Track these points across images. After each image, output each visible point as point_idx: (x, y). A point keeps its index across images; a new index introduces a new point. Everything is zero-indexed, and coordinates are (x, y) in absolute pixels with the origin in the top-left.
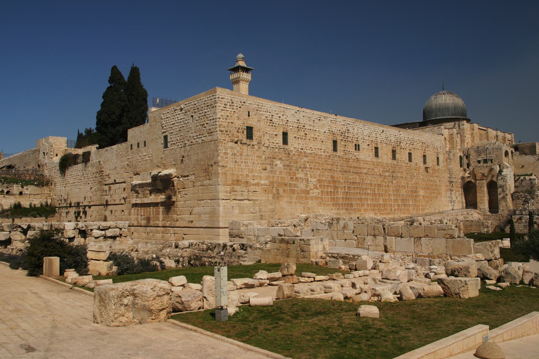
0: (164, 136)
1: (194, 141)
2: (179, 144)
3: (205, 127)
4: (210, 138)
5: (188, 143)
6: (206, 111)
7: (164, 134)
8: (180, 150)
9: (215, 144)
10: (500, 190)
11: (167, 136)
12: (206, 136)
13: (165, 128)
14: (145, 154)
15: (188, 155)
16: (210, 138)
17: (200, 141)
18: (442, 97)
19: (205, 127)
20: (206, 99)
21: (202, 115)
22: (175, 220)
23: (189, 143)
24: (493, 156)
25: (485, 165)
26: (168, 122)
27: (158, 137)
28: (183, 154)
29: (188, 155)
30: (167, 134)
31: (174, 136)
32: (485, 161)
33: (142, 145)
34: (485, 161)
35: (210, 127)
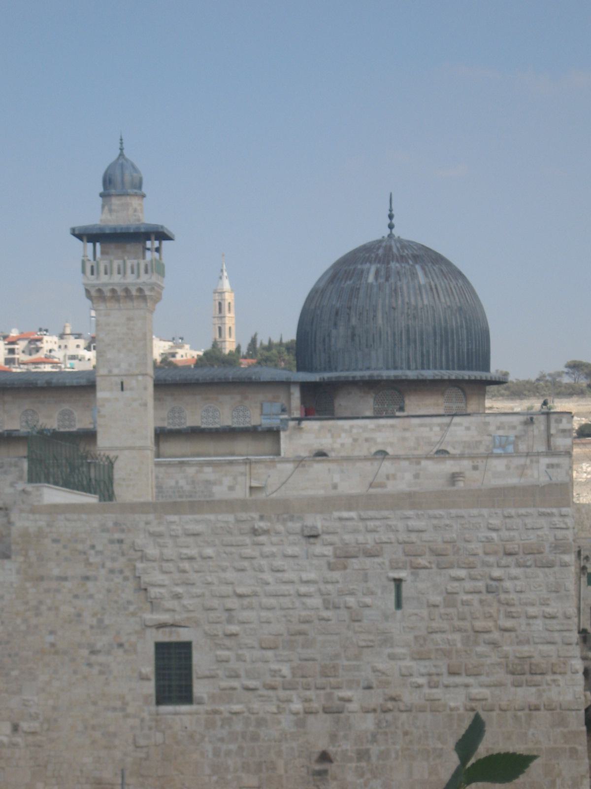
0: (161, 647)
1: (409, 697)
2: (293, 694)
3: (494, 644)
4: (525, 695)
6: (497, 573)
7: (164, 637)
8: (301, 723)
9: (562, 722)
11: (185, 648)
12: (499, 685)
13: (169, 604)
15: (363, 755)
16: (525, 695)
18: (414, 275)
19: (494, 644)
20: (495, 522)
21: (469, 585)
23: (376, 699)
26: (193, 577)
27: (102, 642)
28: (322, 744)
29: (363, 755)
30: (183, 635)
31: (247, 654)
35: (526, 650)
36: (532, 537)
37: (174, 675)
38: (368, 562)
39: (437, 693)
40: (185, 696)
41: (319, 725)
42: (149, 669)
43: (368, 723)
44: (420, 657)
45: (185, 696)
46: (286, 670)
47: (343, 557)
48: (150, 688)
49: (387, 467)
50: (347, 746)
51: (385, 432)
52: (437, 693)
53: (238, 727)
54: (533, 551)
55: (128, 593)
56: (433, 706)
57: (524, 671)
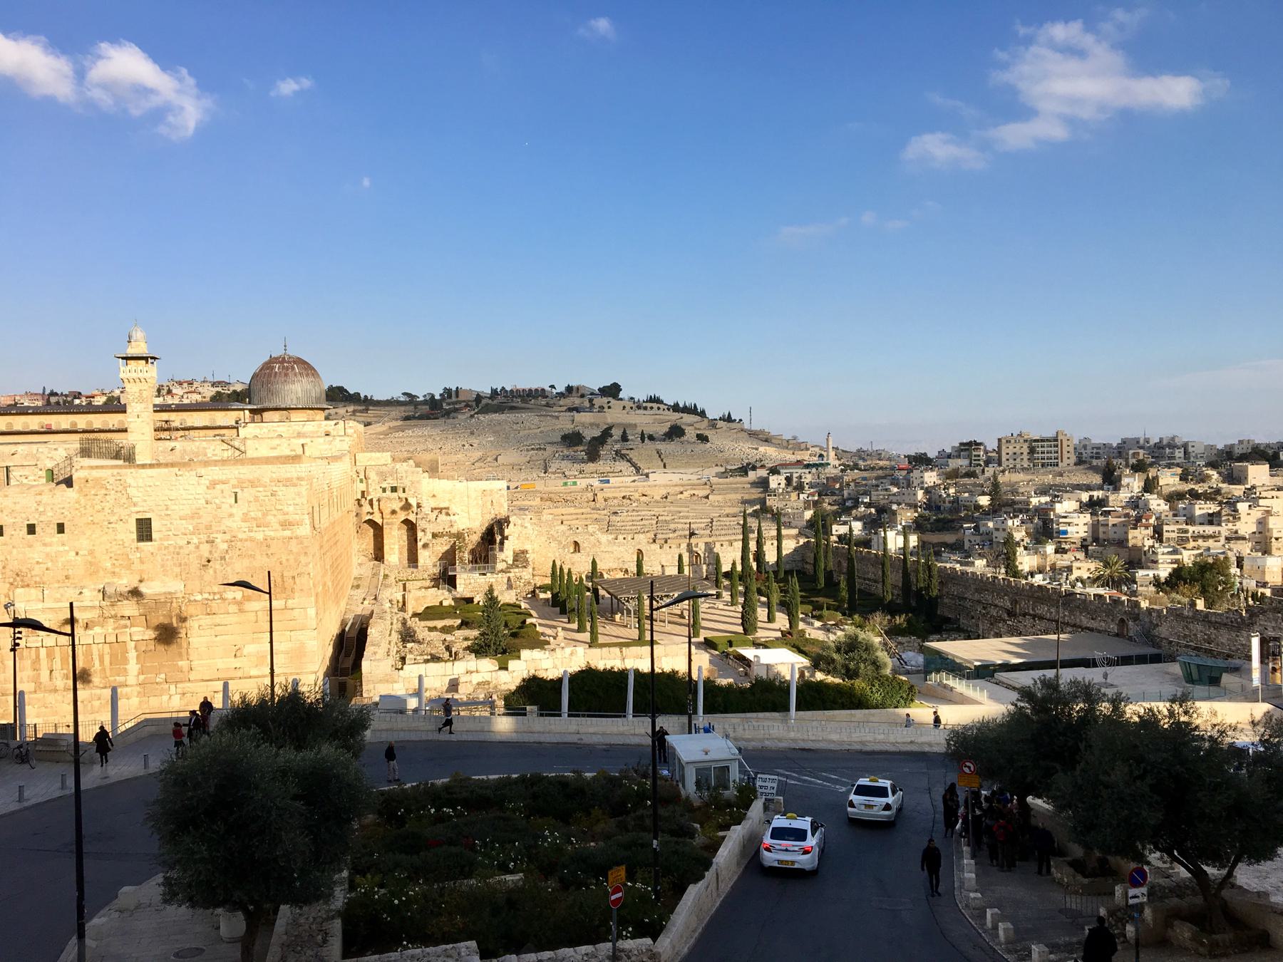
4: (287, 533)
5: (219, 538)
10: (420, 534)
14: (61, 549)
15: (223, 558)
16: (287, 533)
17: (260, 536)
18: (293, 368)
22: (186, 669)
23: (227, 537)
24: (407, 483)
25: (395, 494)
27: (113, 519)
28: (206, 555)
29: (223, 558)
30: (147, 516)
32: (394, 489)
33: (47, 533)
34: (394, 489)
36: (289, 475)
37: (144, 530)
38: (223, 486)
39: (252, 534)
40: (150, 539)
41: (205, 548)
42: (134, 529)
43: (225, 546)
44: (244, 521)
45: (150, 539)
46: (191, 528)
47: (213, 484)
48: (134, 536)
49: (277, 441)
50: (216, 555)
51: (283, 428)
52: (252, 534)
53: (172, 549)
54: (288, 480)
55: (124, 500)
56: (252, 540)
57: (286, 525)
